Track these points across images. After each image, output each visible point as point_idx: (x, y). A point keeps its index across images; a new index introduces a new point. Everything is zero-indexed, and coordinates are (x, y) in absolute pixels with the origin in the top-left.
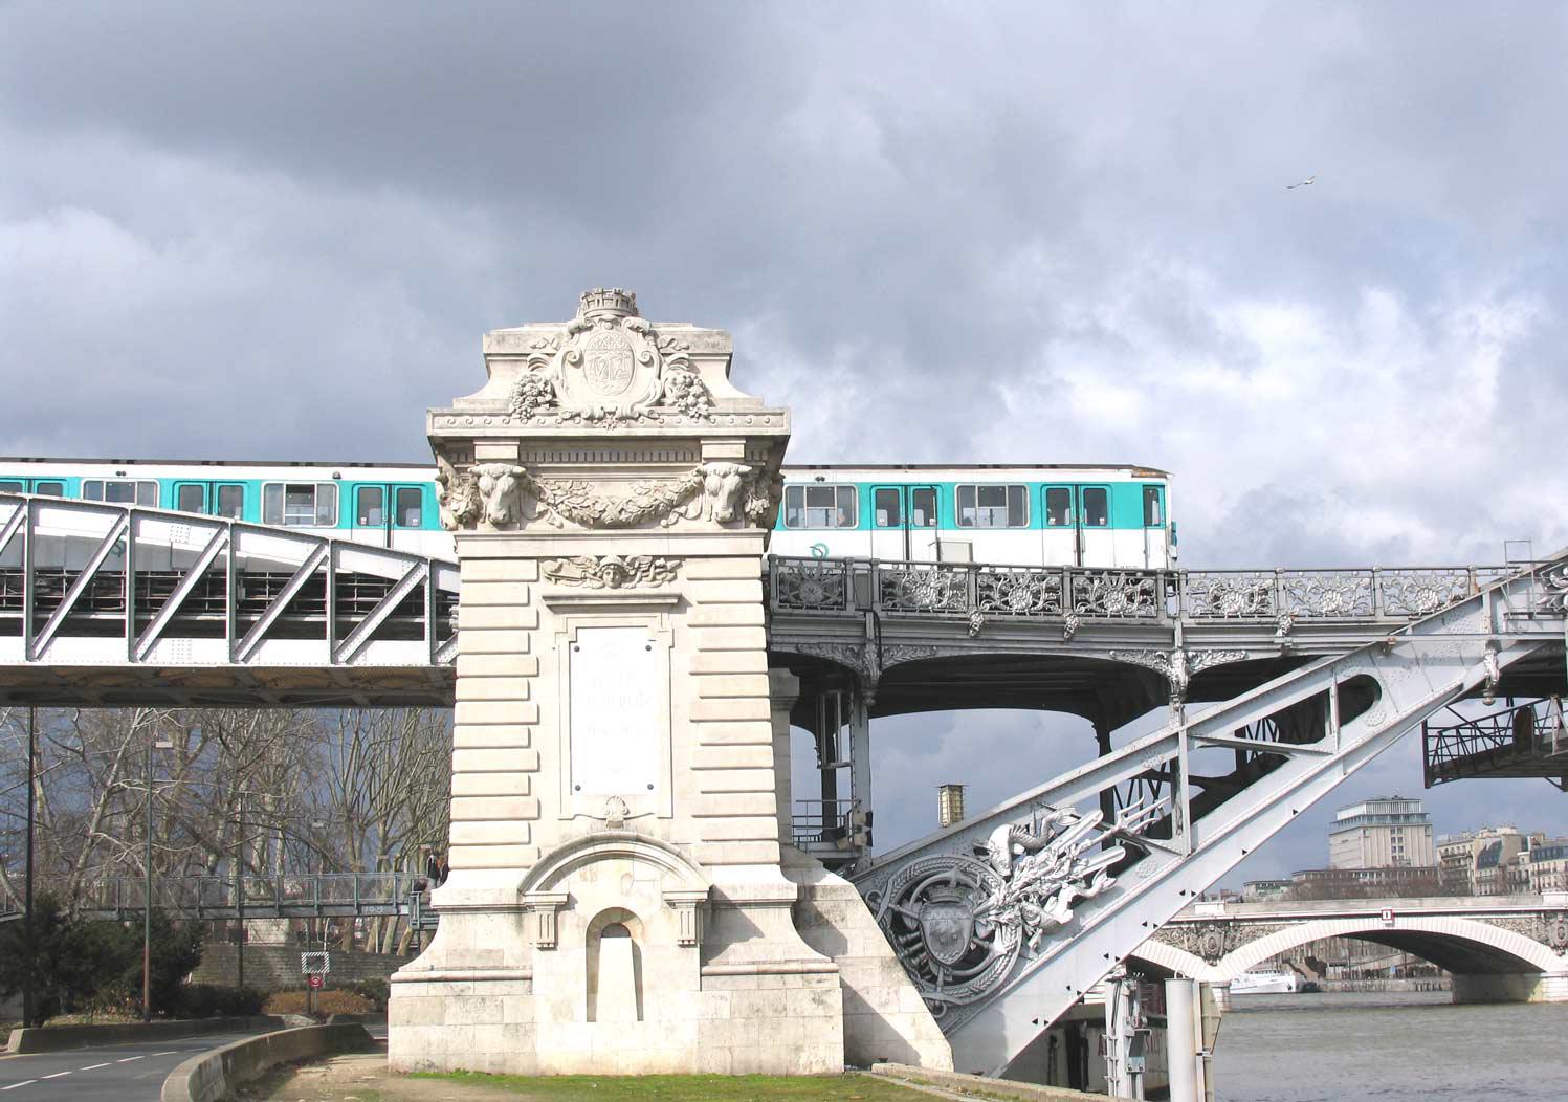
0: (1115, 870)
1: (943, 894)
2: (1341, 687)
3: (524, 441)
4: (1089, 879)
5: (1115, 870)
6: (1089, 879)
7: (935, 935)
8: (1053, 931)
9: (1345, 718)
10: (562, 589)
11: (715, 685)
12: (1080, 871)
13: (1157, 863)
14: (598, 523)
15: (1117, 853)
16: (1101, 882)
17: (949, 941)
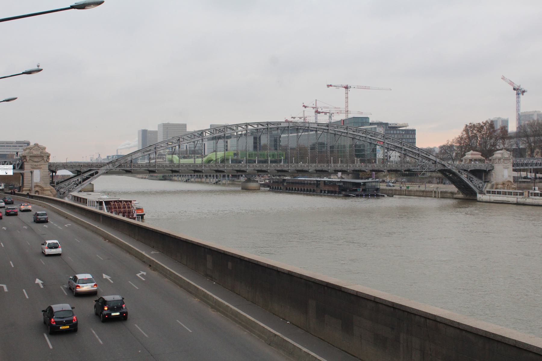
0: (76, 186)
1: (62, 188)
2: (95, 172)
3: (30, 156)
4: (74, 187)
5: (76, 186)
6: (74, 187)
7: (61, 191)
8: (71, 191)
9: (95, 174)
10: (33, 167)
11: (44, 174)
12: (73, 186)
13: (79, 186)
14: (35, 162)
15: (76, 185)
16: (75, 187)
17: (62, 192)
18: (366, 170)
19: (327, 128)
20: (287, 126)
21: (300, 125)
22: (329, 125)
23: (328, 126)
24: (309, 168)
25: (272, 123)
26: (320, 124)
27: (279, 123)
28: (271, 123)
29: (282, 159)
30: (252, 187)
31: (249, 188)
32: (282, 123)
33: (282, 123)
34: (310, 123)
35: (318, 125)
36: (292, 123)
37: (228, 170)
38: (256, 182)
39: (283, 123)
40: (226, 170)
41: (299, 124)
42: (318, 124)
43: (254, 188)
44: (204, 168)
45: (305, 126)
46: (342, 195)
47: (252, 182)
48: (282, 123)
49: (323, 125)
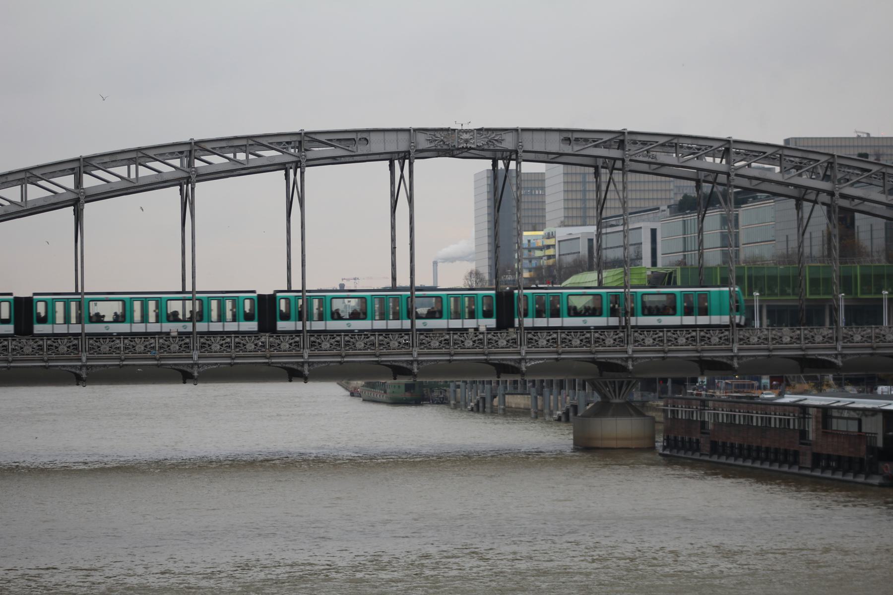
18: (836, 356)
19: (615, 153)
20: (403, 147)
21: (467, 141)
22: (628, 137)
23: (621, 145)
24: (519, 353)
25: (323, 138)
26: (576, 135)
27: (360, 136)
28: (313, 136)
29: (881, 300)
30: (617, 439)
31: (599, 444)
32: (372, 134)
33: (373, 137)
34: (524, 130)
35: (568, 140)
36: (428, 136)
37: (94, 370)
38: (631, 415)
39: (381, 135)
40: (84, 369)
41: (465, 136)
42: (569, 135)
43: (621, 444)
44: (88, 359)
45: (499, 146)
46: (876, 480)
47: (613, 416)
48: (373, 137)
49: (586, 140)
